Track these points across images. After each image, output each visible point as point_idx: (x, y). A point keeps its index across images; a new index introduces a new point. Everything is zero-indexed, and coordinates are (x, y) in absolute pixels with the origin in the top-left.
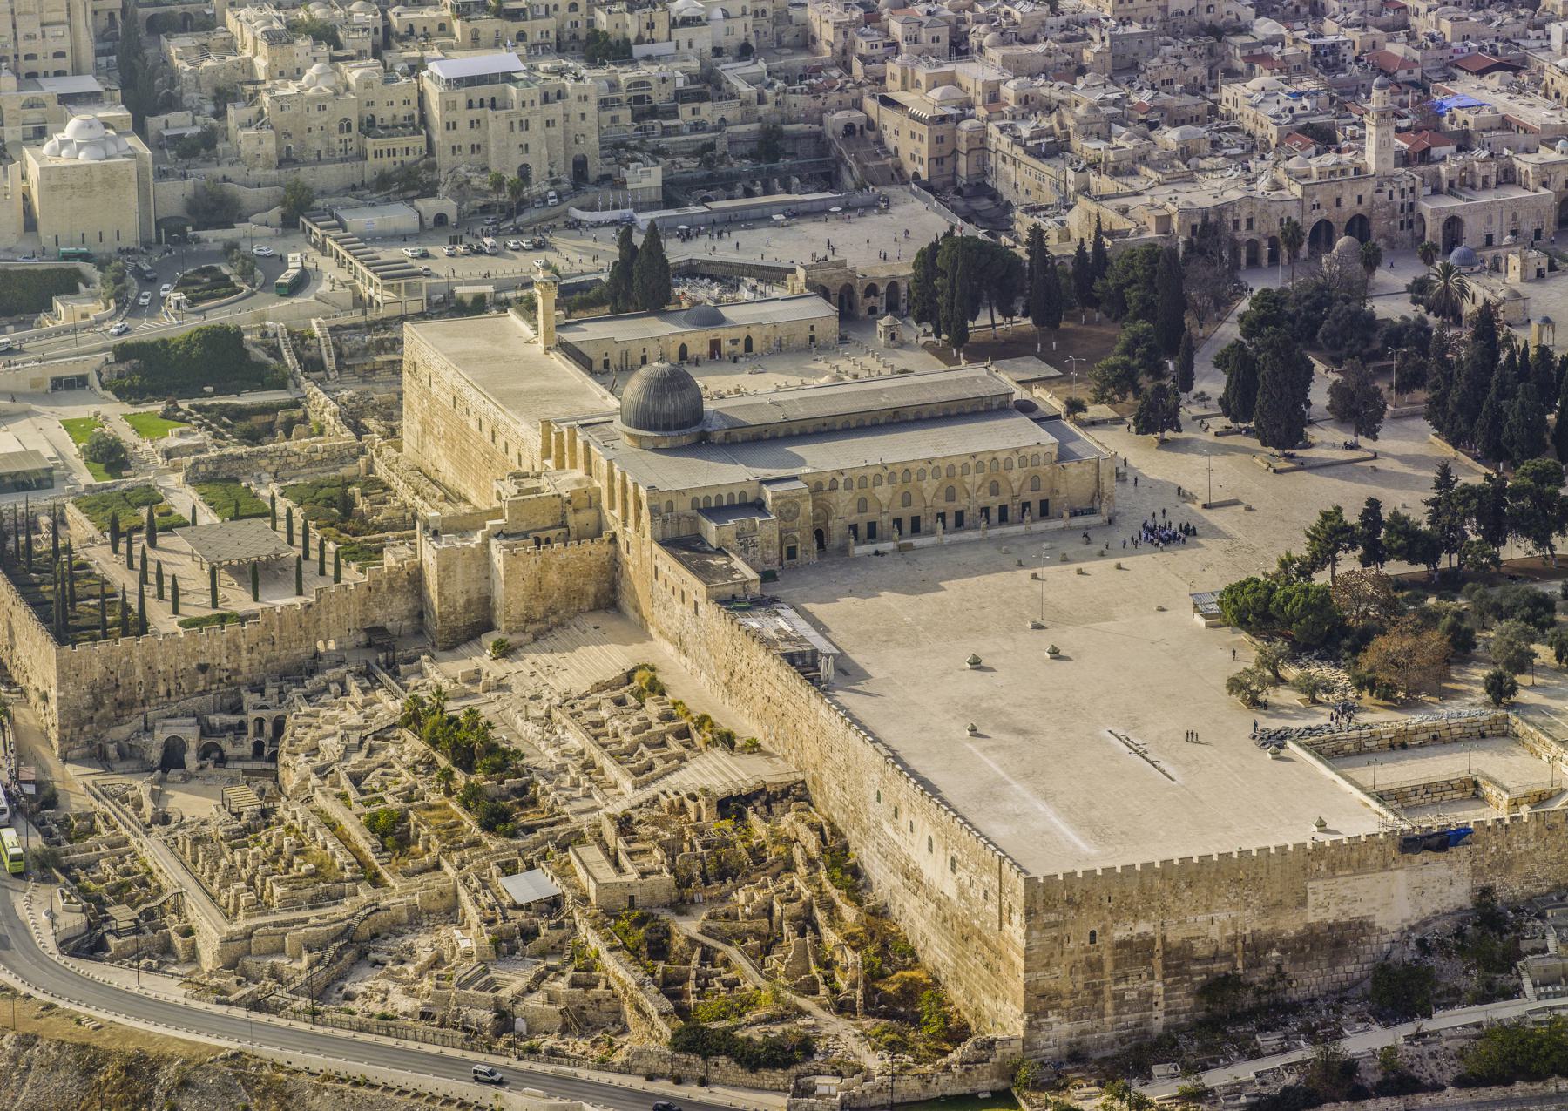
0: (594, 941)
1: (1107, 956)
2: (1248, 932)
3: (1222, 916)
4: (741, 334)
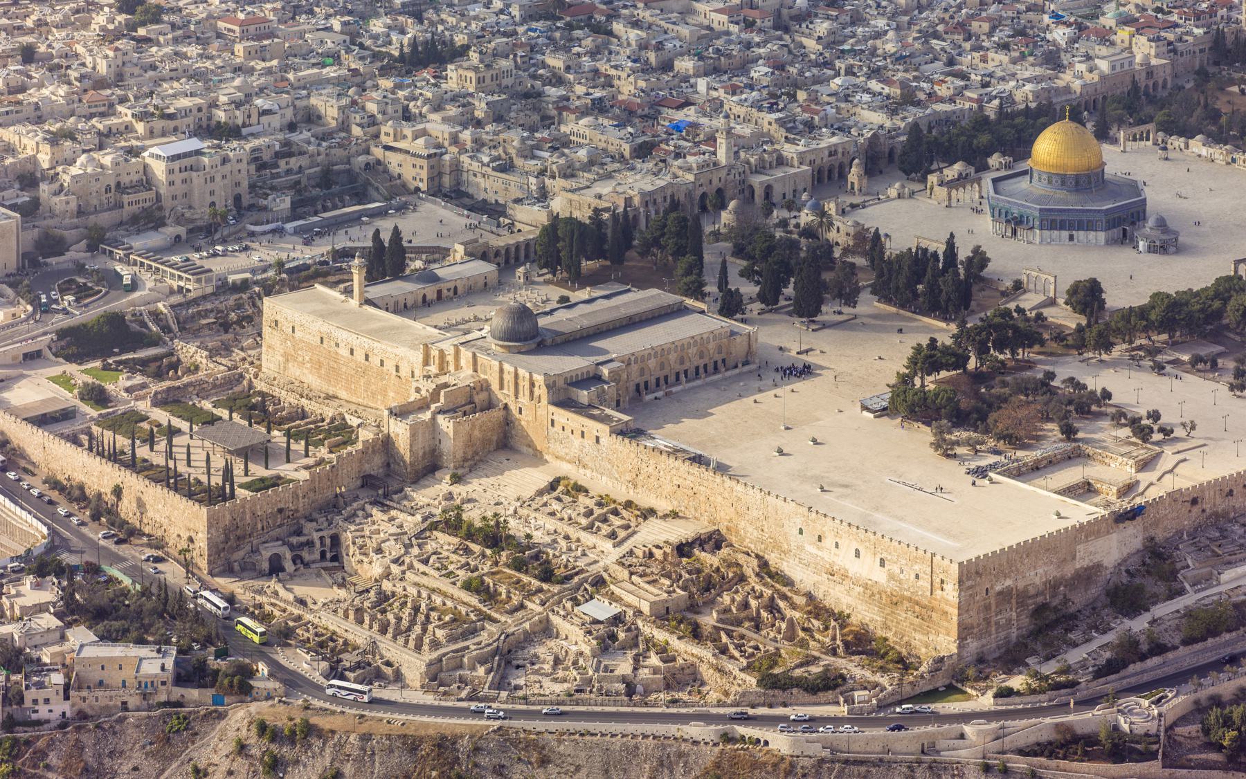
0: (660, 636)
1: (993, 602)
4: (451, 285)
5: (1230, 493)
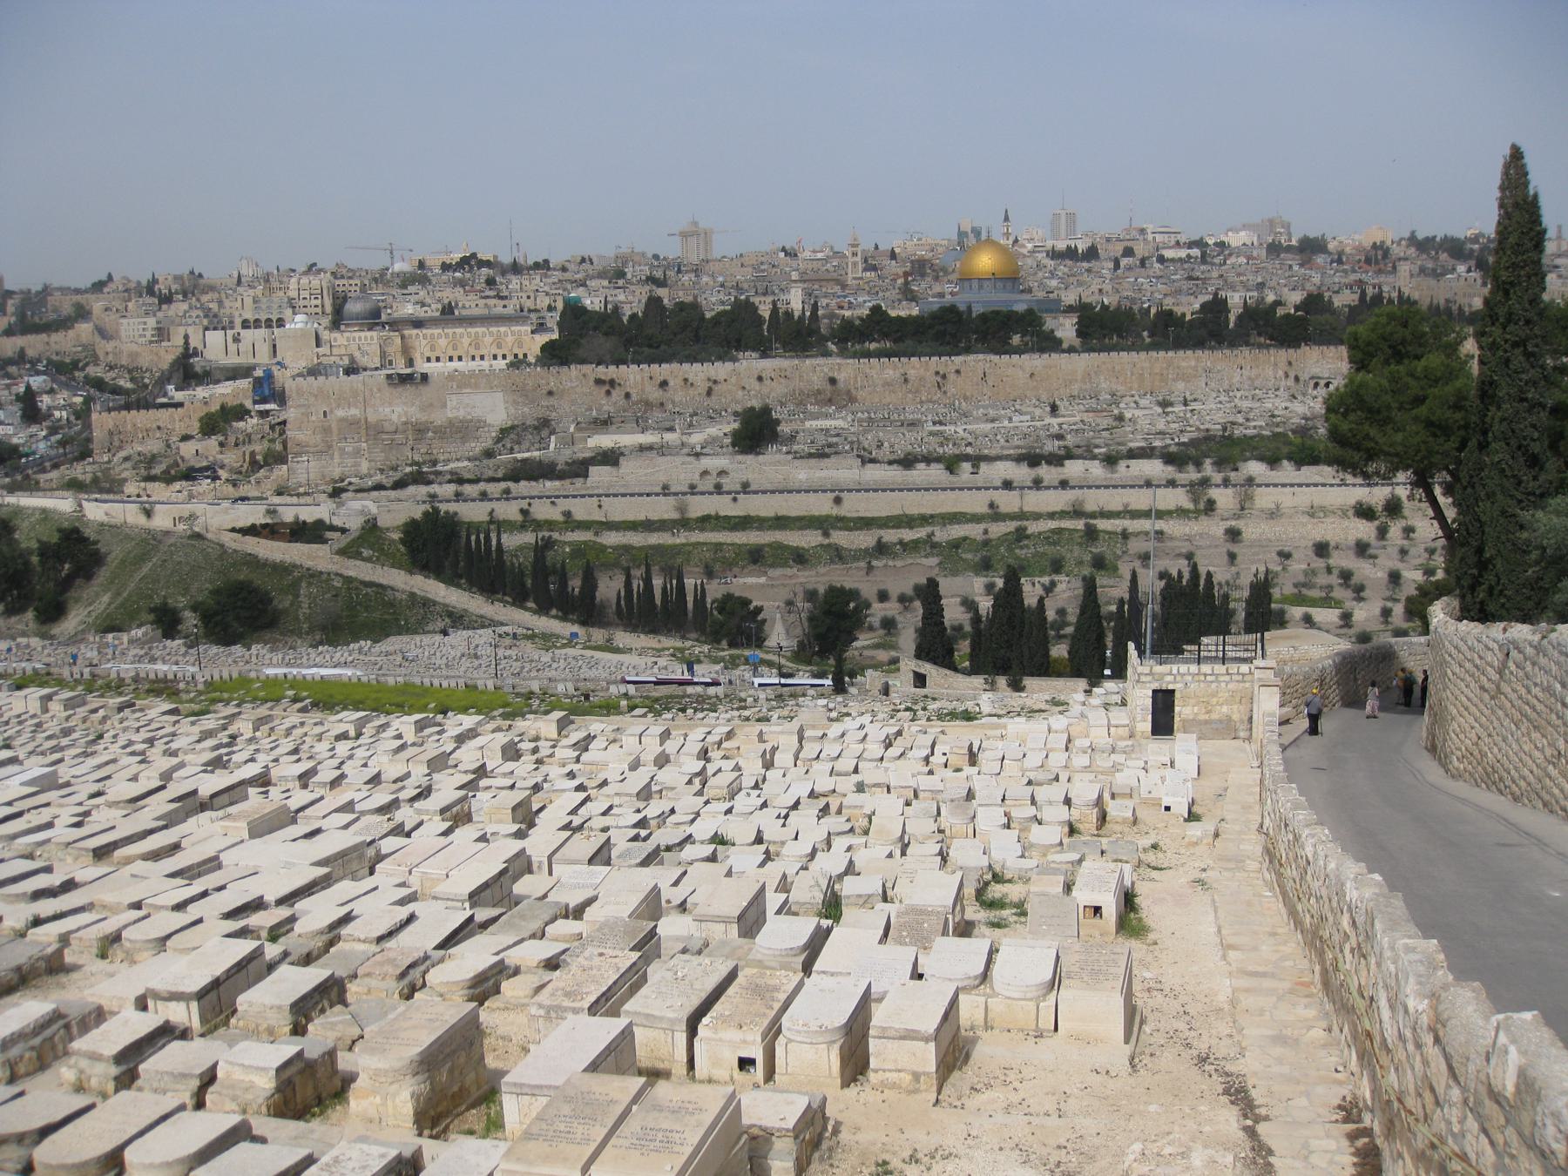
3: (398, 410)
5: (664, 384)
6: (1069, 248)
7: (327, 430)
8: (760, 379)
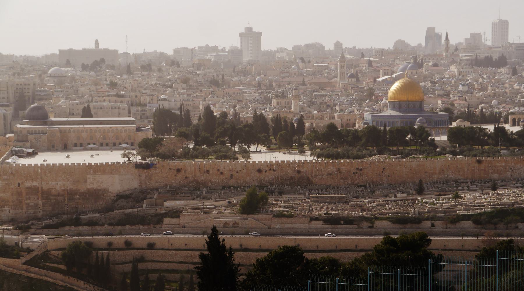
2: (69, 188)
6: (486, 58)
7: (20, 194)
8: (260, 171)
